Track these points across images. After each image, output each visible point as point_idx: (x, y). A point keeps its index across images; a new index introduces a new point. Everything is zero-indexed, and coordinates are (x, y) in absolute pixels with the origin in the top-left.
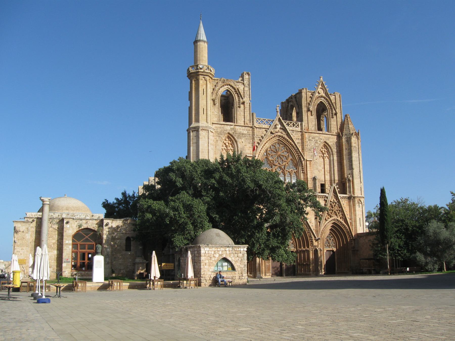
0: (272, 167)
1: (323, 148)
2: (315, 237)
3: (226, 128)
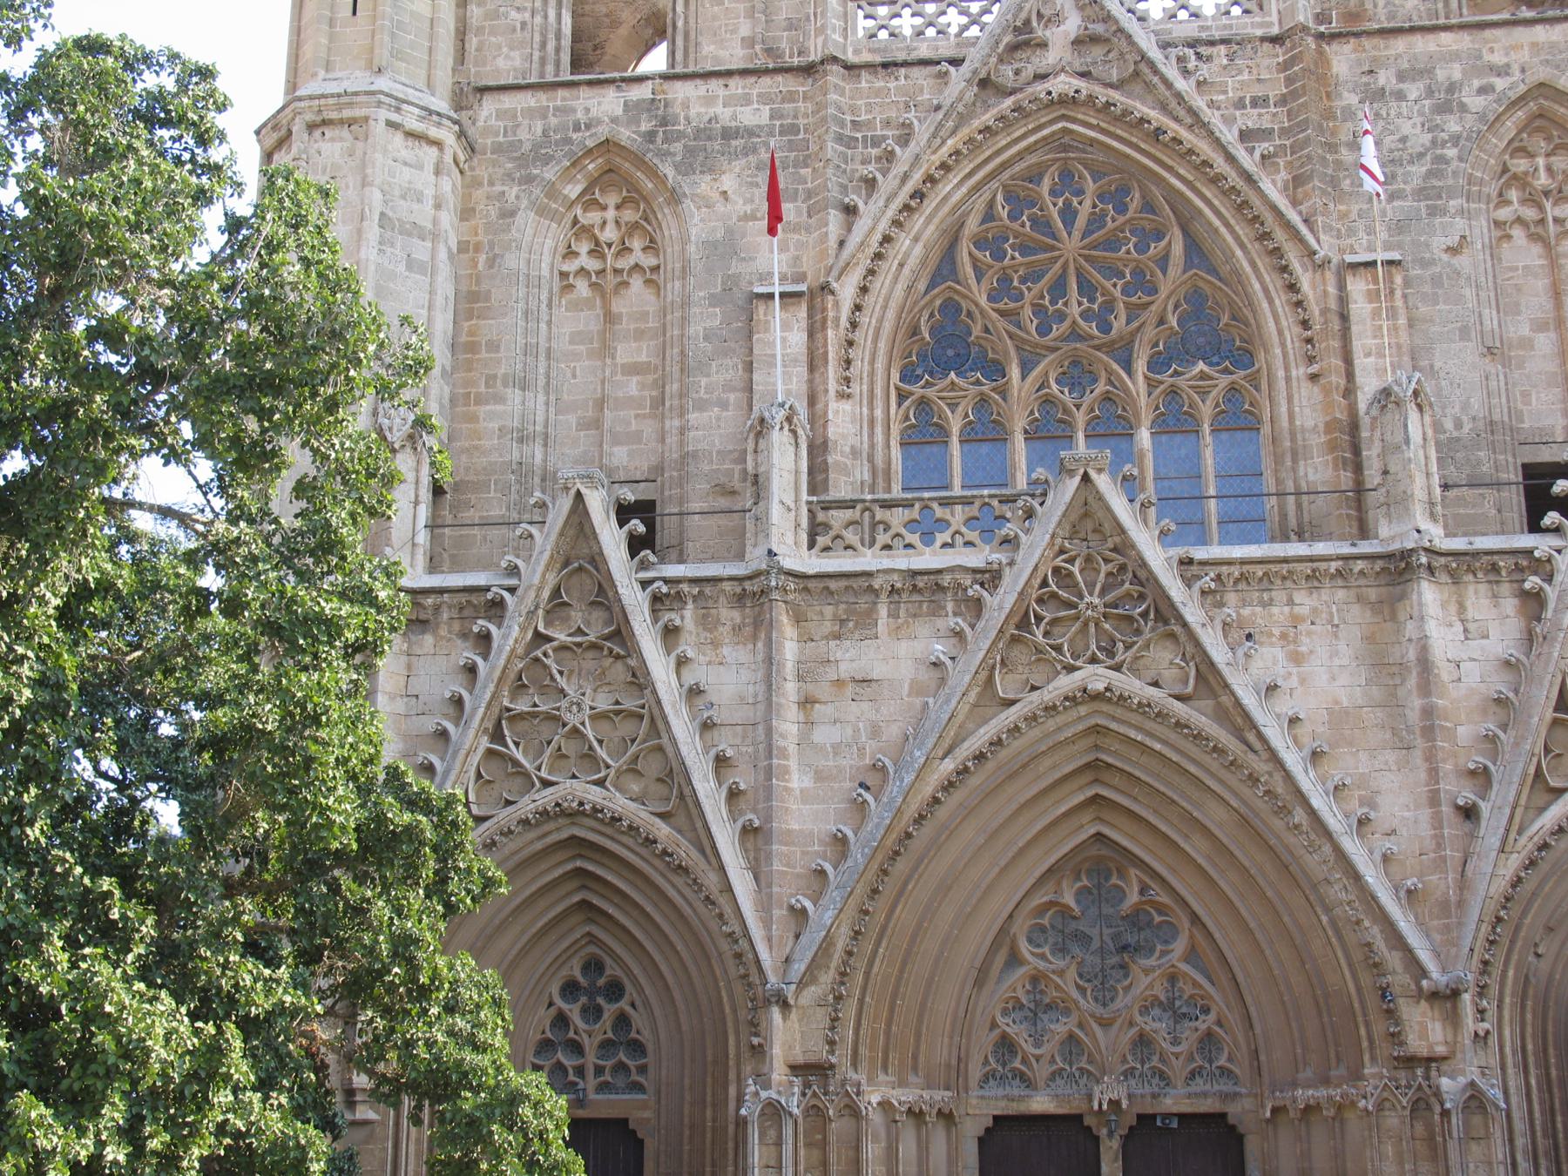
0: (996, 370)
1: (1532, 156)
2: (1424, 973)
3: (587, 110)
